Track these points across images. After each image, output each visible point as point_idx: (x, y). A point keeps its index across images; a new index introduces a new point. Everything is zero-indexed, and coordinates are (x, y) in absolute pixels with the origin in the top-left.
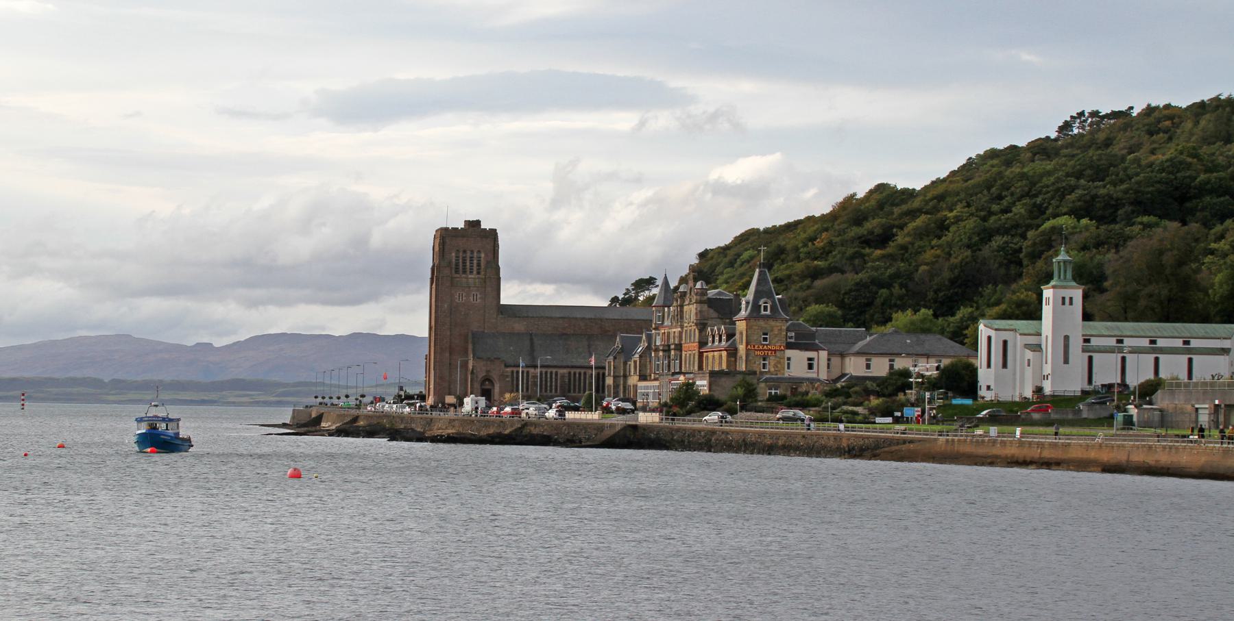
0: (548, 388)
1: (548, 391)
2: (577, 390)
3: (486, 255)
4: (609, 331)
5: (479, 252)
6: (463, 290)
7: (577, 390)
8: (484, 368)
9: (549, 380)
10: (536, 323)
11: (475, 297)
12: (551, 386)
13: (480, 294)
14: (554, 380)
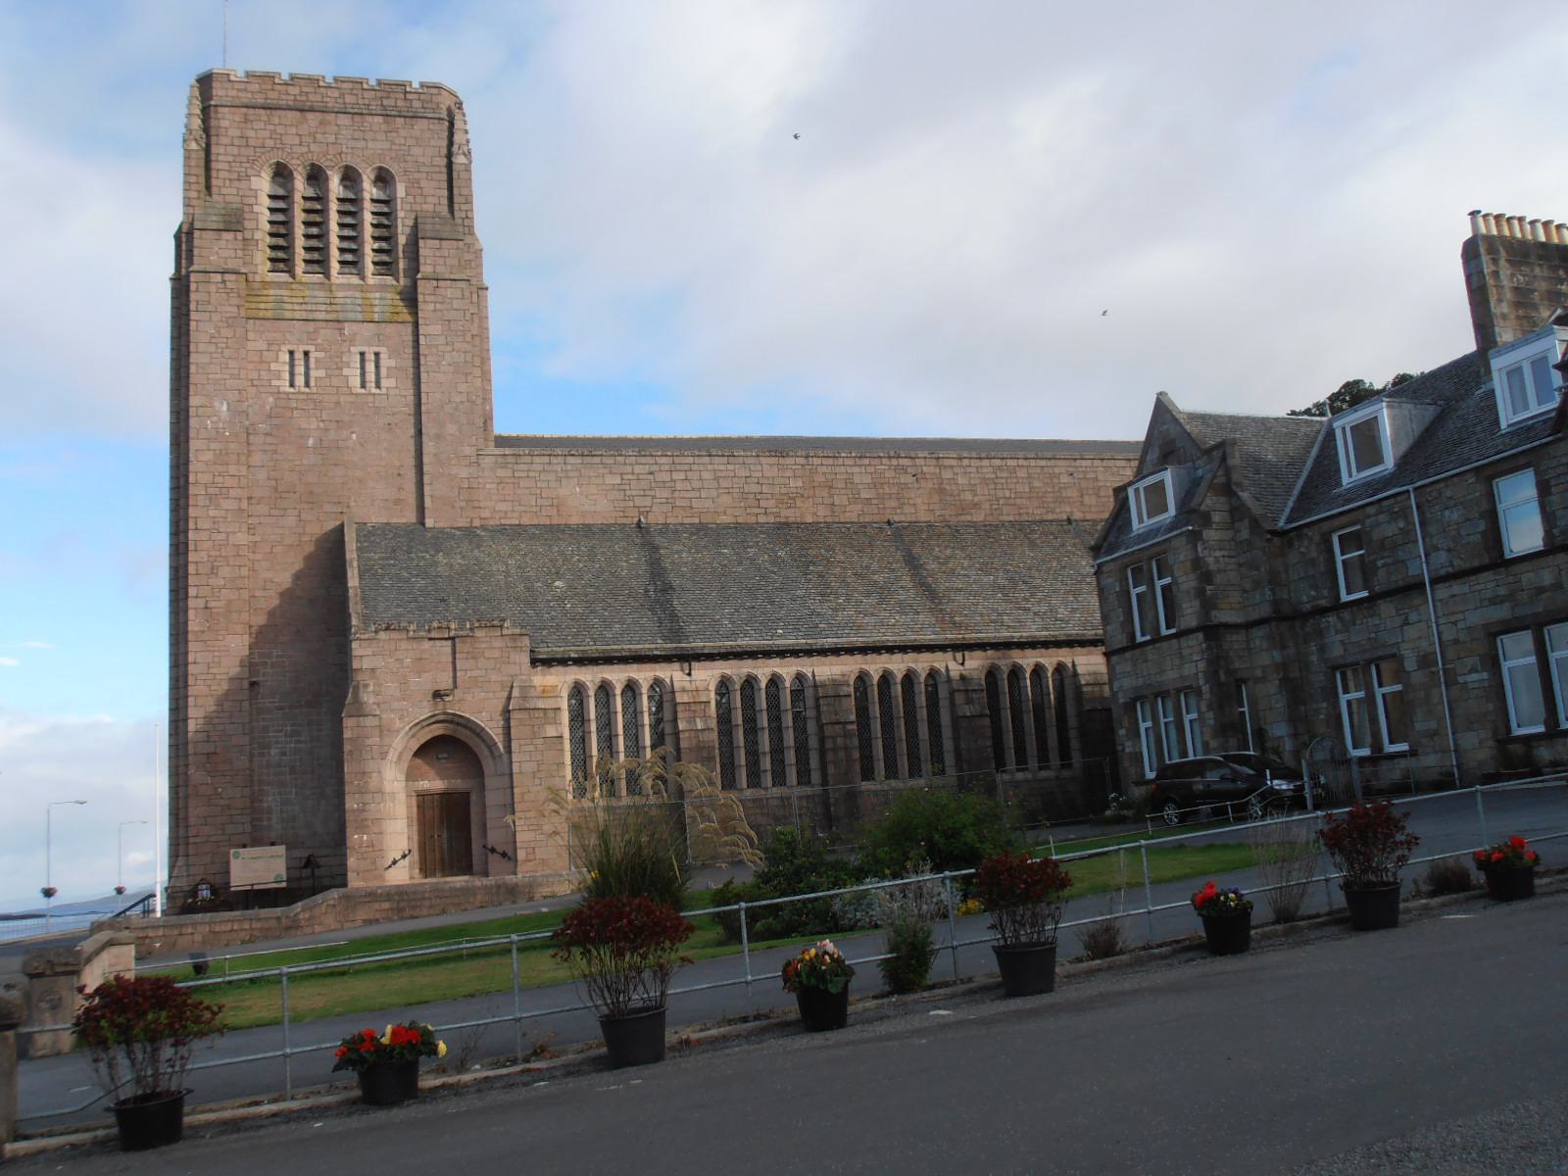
0: (766, 763)
1: (768, 780)
2: (903, 763)
3: (413, 185)
4: (976, 505)
5: (383, 178)
6: (311, 337)
7: (903, 763)
8: (424, 683)
9: (763, 720)
10: (666, 477)
11: (370, 367)
12: (778, 751)
13: (394, 353)
14: (788, 720)
